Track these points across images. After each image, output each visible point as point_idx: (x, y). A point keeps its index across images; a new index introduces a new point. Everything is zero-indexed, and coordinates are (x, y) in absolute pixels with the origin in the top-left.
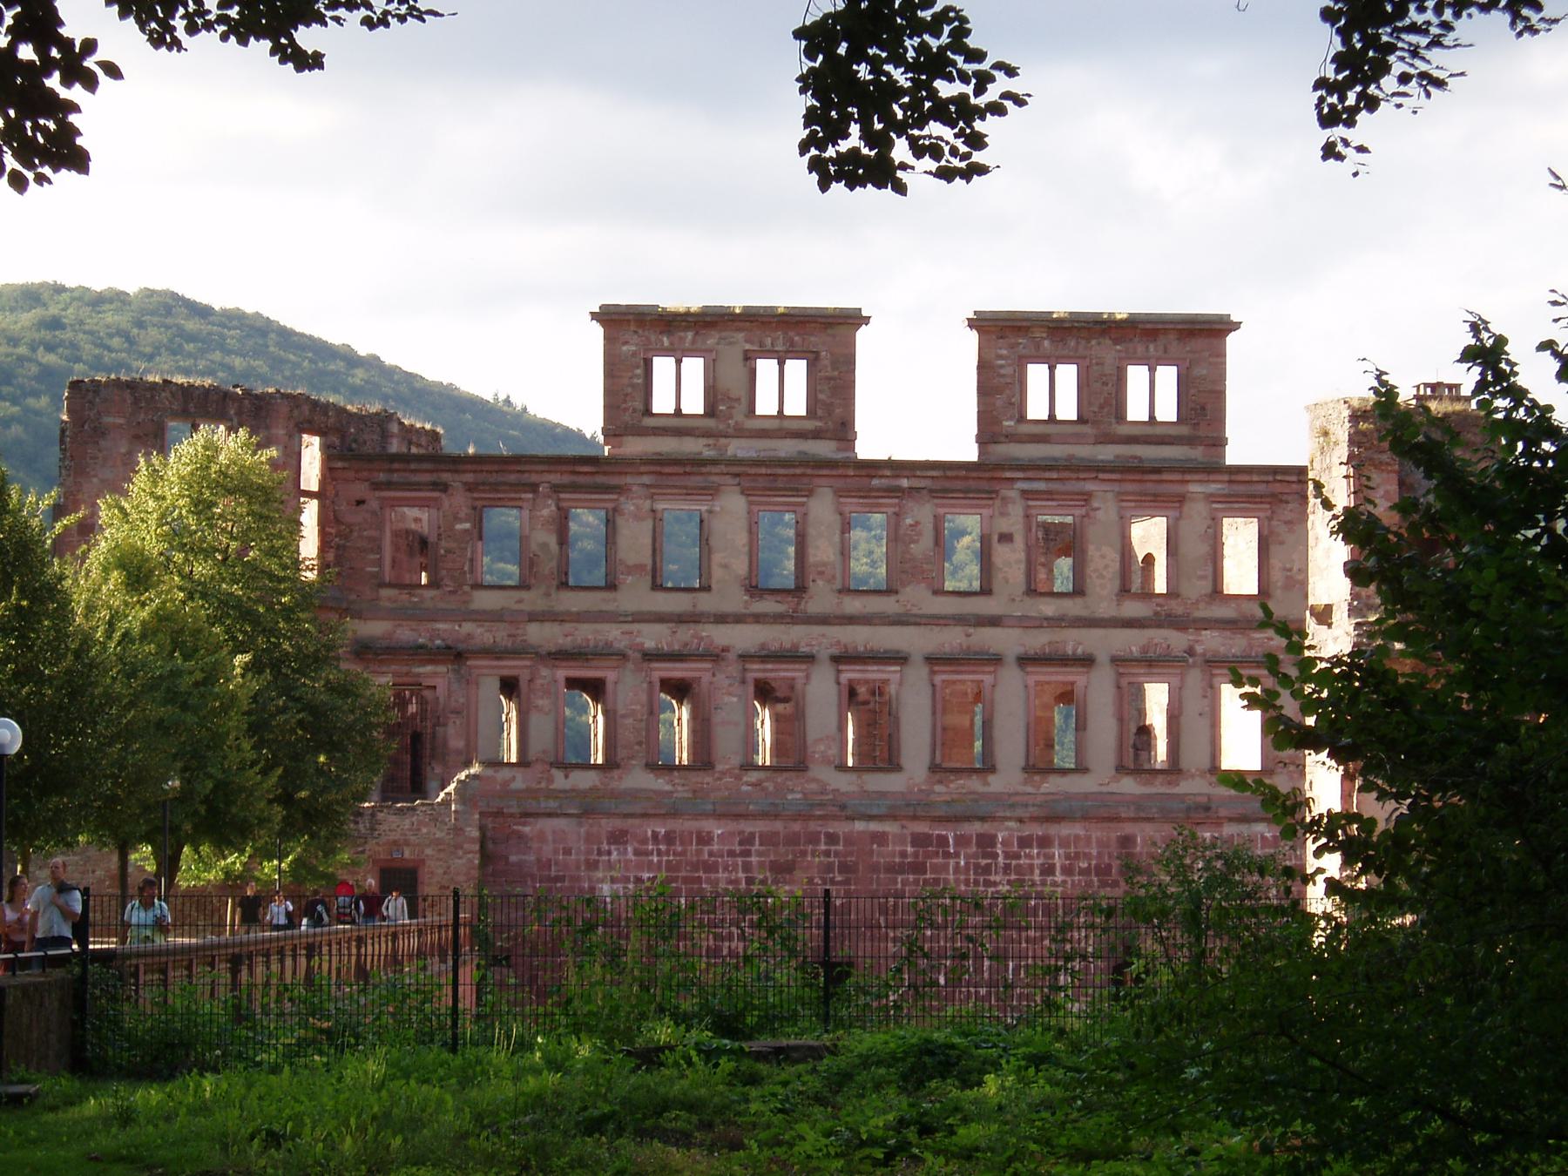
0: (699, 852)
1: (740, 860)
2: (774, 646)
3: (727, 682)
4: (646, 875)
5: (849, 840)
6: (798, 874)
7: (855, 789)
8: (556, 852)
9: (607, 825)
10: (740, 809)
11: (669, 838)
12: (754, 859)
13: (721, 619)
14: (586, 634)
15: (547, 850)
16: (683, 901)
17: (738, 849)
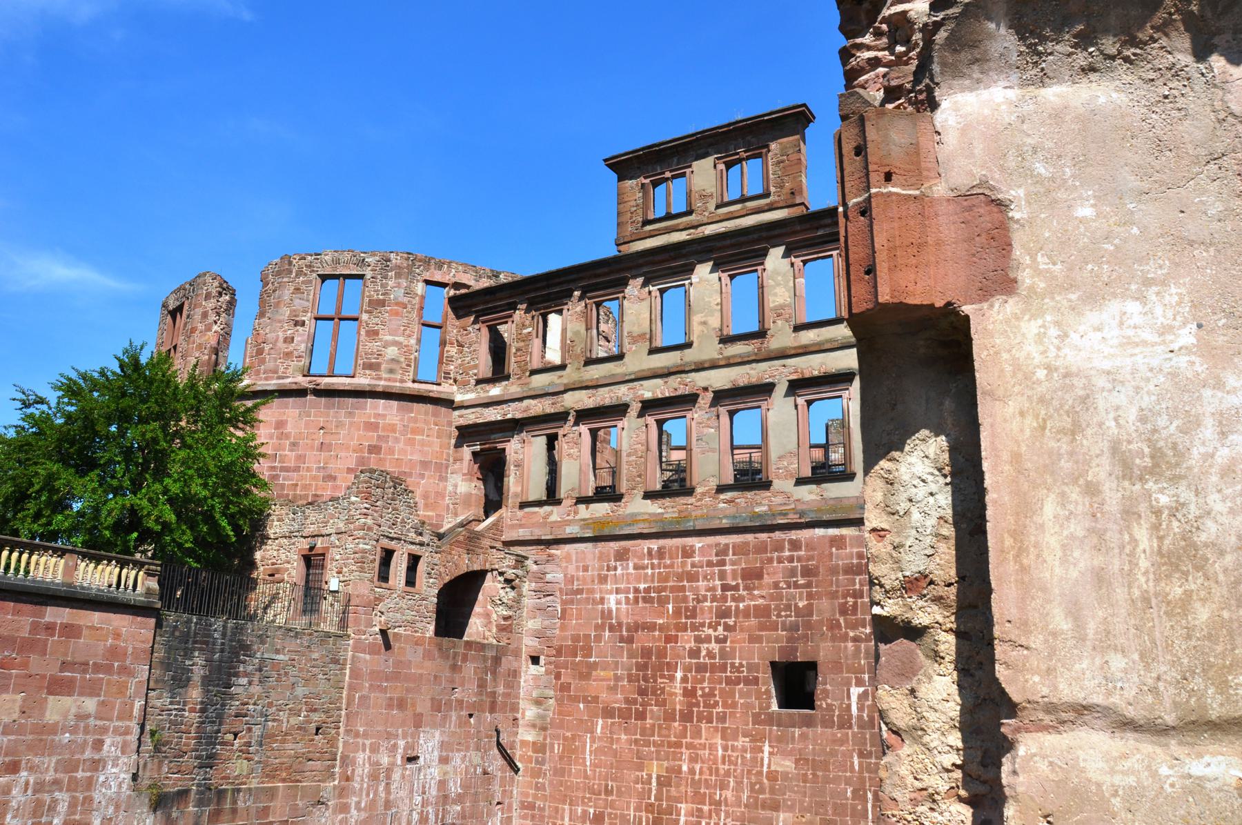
0: (684, 564)
1: (716, 569)
2: (742, 382)
3: (707, 416)
4: (642, 586)
5: (810, 546)
6: (767, 579)
7: (813, 497)
8: (578, 568)
9: (615, 545)
10: (715, 524)
11: (661, 553)
12: (728, 568)
13: (700, 368)
14: (605, 397)
15: (572, 570)
16: (670, 606)
17: (715, 559)
